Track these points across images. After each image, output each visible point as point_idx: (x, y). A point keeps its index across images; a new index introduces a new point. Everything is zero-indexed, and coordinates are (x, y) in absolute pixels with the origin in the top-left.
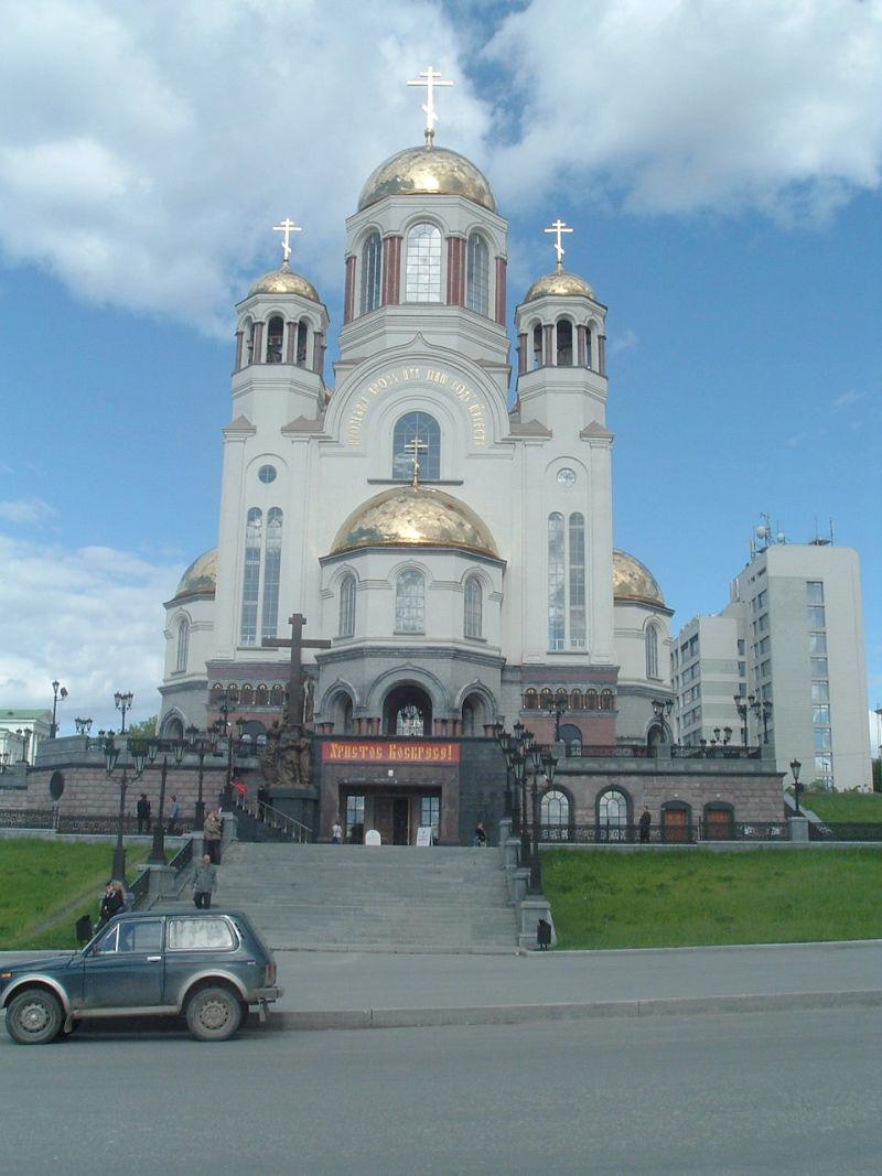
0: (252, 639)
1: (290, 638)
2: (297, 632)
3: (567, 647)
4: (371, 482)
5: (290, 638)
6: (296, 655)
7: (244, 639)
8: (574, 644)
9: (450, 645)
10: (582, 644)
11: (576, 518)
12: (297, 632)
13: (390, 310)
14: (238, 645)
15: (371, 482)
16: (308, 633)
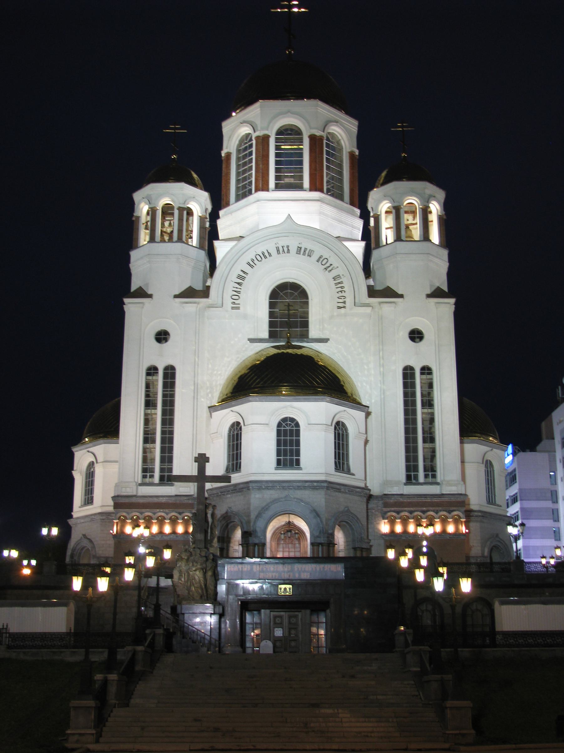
0: (152, 476)
1: (196, 474)
2: (202, 470)
3: (421, 479)
4: (252, 340)
5: (196, 474)
6: (201, 489)
7: (144, 477)
8: (426, 476)
9: (323, 478)
10: (434, 476)
11: (426, 370)
12: (202, 470)
13: (262, 194)
14: (140, 482)
15: (252, 340)
16: (210, 470)
